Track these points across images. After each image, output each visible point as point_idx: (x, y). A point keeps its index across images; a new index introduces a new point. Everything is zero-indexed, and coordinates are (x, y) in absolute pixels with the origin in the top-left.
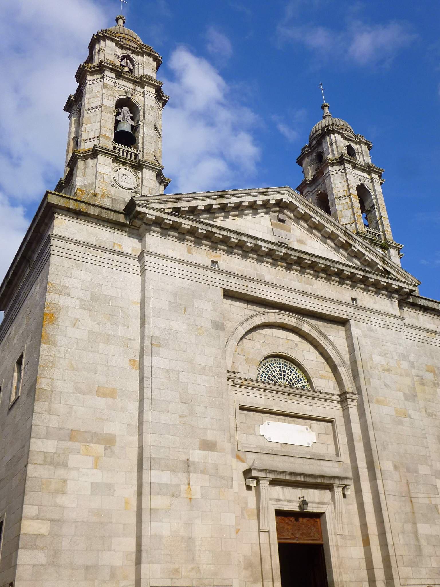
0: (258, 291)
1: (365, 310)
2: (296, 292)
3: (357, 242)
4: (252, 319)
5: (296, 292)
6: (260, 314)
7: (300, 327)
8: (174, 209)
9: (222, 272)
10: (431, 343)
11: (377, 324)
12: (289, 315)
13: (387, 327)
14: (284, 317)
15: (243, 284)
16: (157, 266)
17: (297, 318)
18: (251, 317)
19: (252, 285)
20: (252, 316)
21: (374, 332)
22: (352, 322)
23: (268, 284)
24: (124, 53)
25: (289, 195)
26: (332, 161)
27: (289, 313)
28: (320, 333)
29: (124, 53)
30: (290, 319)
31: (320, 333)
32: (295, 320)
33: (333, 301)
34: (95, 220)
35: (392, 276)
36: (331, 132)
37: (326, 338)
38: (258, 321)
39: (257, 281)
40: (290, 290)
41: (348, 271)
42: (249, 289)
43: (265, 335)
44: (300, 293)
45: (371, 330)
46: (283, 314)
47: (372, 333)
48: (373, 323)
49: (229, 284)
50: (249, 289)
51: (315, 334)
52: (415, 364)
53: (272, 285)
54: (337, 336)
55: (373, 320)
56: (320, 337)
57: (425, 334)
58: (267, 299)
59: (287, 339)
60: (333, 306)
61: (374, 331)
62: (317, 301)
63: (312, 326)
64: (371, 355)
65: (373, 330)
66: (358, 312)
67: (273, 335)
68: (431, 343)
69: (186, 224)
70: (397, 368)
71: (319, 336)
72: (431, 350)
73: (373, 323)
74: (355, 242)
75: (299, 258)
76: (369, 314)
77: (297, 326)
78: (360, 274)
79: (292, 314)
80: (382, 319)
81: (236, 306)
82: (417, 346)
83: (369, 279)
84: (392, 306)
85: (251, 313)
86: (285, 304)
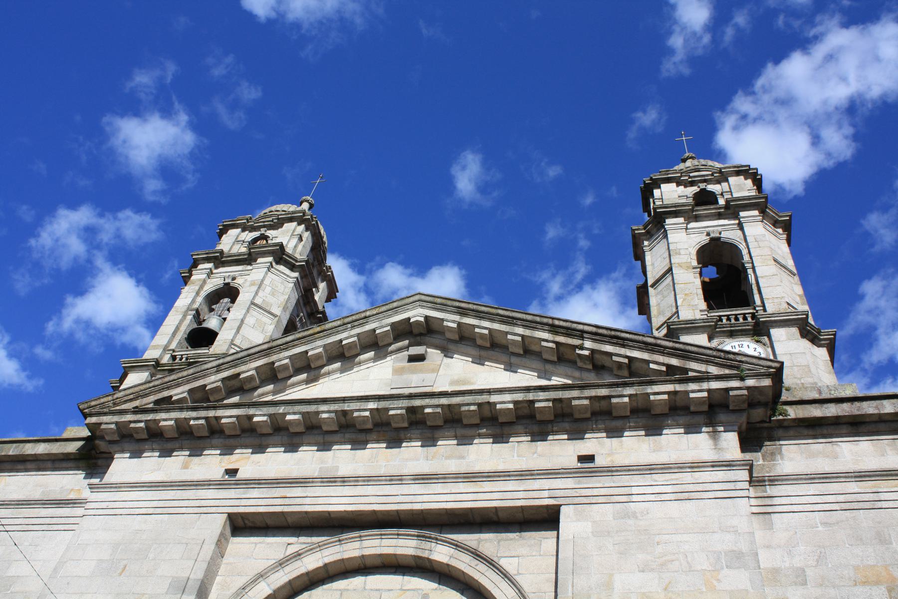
0: (307, 501)
1: (612, 471)
2: (405, 479)
3: (585, 335)
4: (299, 562)
5: (405, 479)
6: (320, 547)
7: (425, 554)
8: (157, 402)
9: (234, 484)
10: (879, 505)
11: (652, 497)
12: (398, 535)
13: (685, 496)
14: (386, 542)
15: (276, 495)
16: (104, 505)
17: (418, 536)
18: (295, 556)
19: (297, 491)
20: (298, 555)
21: (637, 518)
22: (564, 511)
23: (335, 482)
24: (256, 234)
25: (422, 307)
26: (644, 229)
27: (376, 532)
28: (477, 555)
29: (256, 234)
30: (401, 542)
31: (477, 555)
32: (413, 543)
33: (509, 476)
34: (49, 465)
35: (691, 374)
36: (651, 186)
37: (491, 563)
38: (312, 562)
39: (309, 482)
40: (391, 480)
41: (543, 401)
42: (287, 501)
43: (342, 591)
44: (414, 479)
45: (634, 515)
46: (381, 535)
47: (631, 522)
48: (634, 498)
49: (244, 502)
50: (287, 501)
51: (464, 564)
52: (809, 572)
53: (344, 482)
54: (534, 553)
55: (635, 490)
56: (476, 565)
57: (853, 487)
58: (329, 513)
59: (401, 589)
60: (511, 485)
61: (638, 515)
62: (462, 487)
63: (457, 546)
64: (612, 575)
65: (634, 513)
66: (586, 483)
67: (364, 587)
68: (879, 505)
69: (167, 420)
70: (702, 593)
71: (474, 562)
72: (880, 523)
73: (634, 498)
74: (582, 338)
75: (411, 410)
76: (625, 480)
77: (420, 553)
78: (580, 399)
79: (402, 531)
80: (667, 480)
81: (268, 543)
82: (824, 524)
83: (614, 400)
84: (716, 445)
85: (292, 550)
86: (374, 512)
